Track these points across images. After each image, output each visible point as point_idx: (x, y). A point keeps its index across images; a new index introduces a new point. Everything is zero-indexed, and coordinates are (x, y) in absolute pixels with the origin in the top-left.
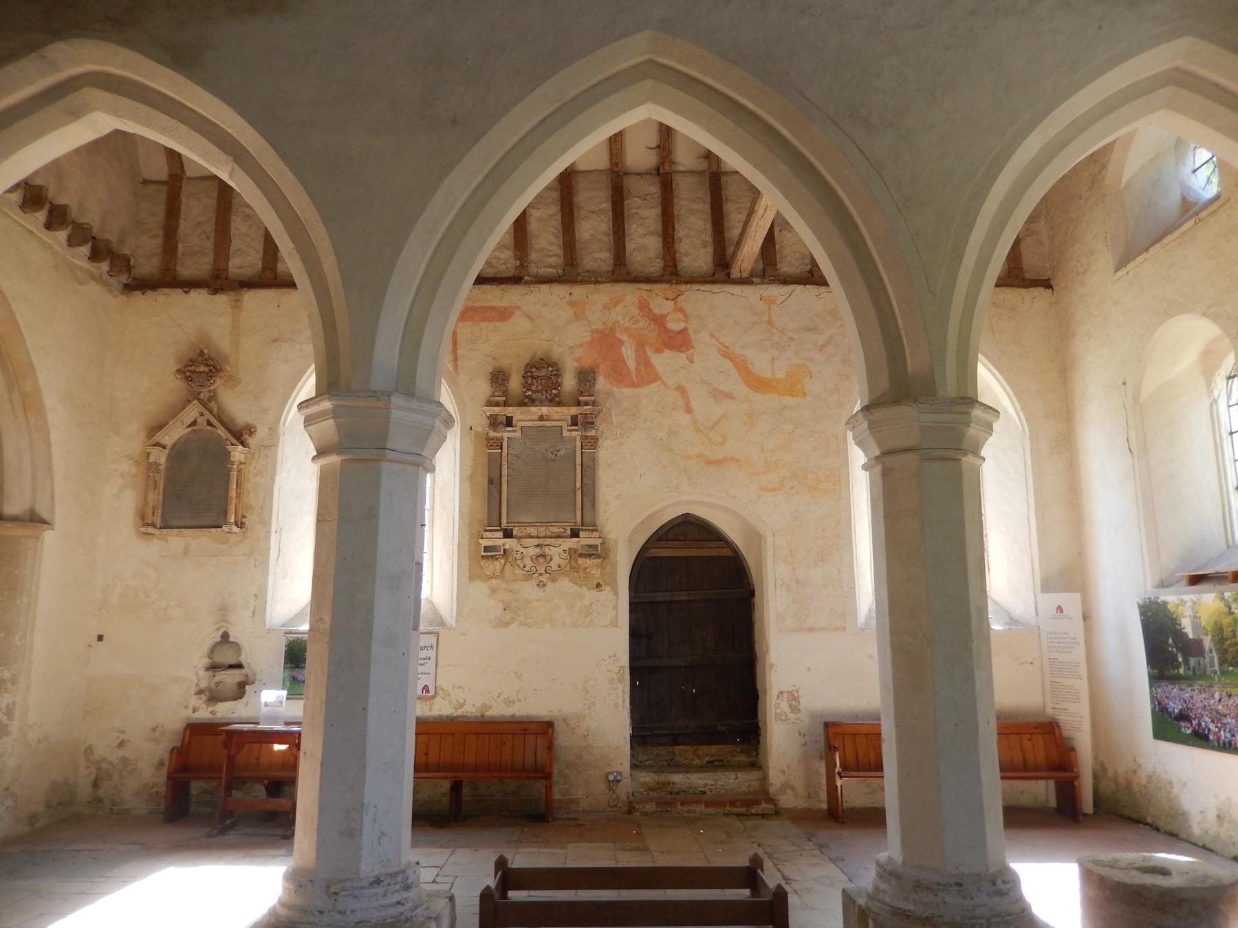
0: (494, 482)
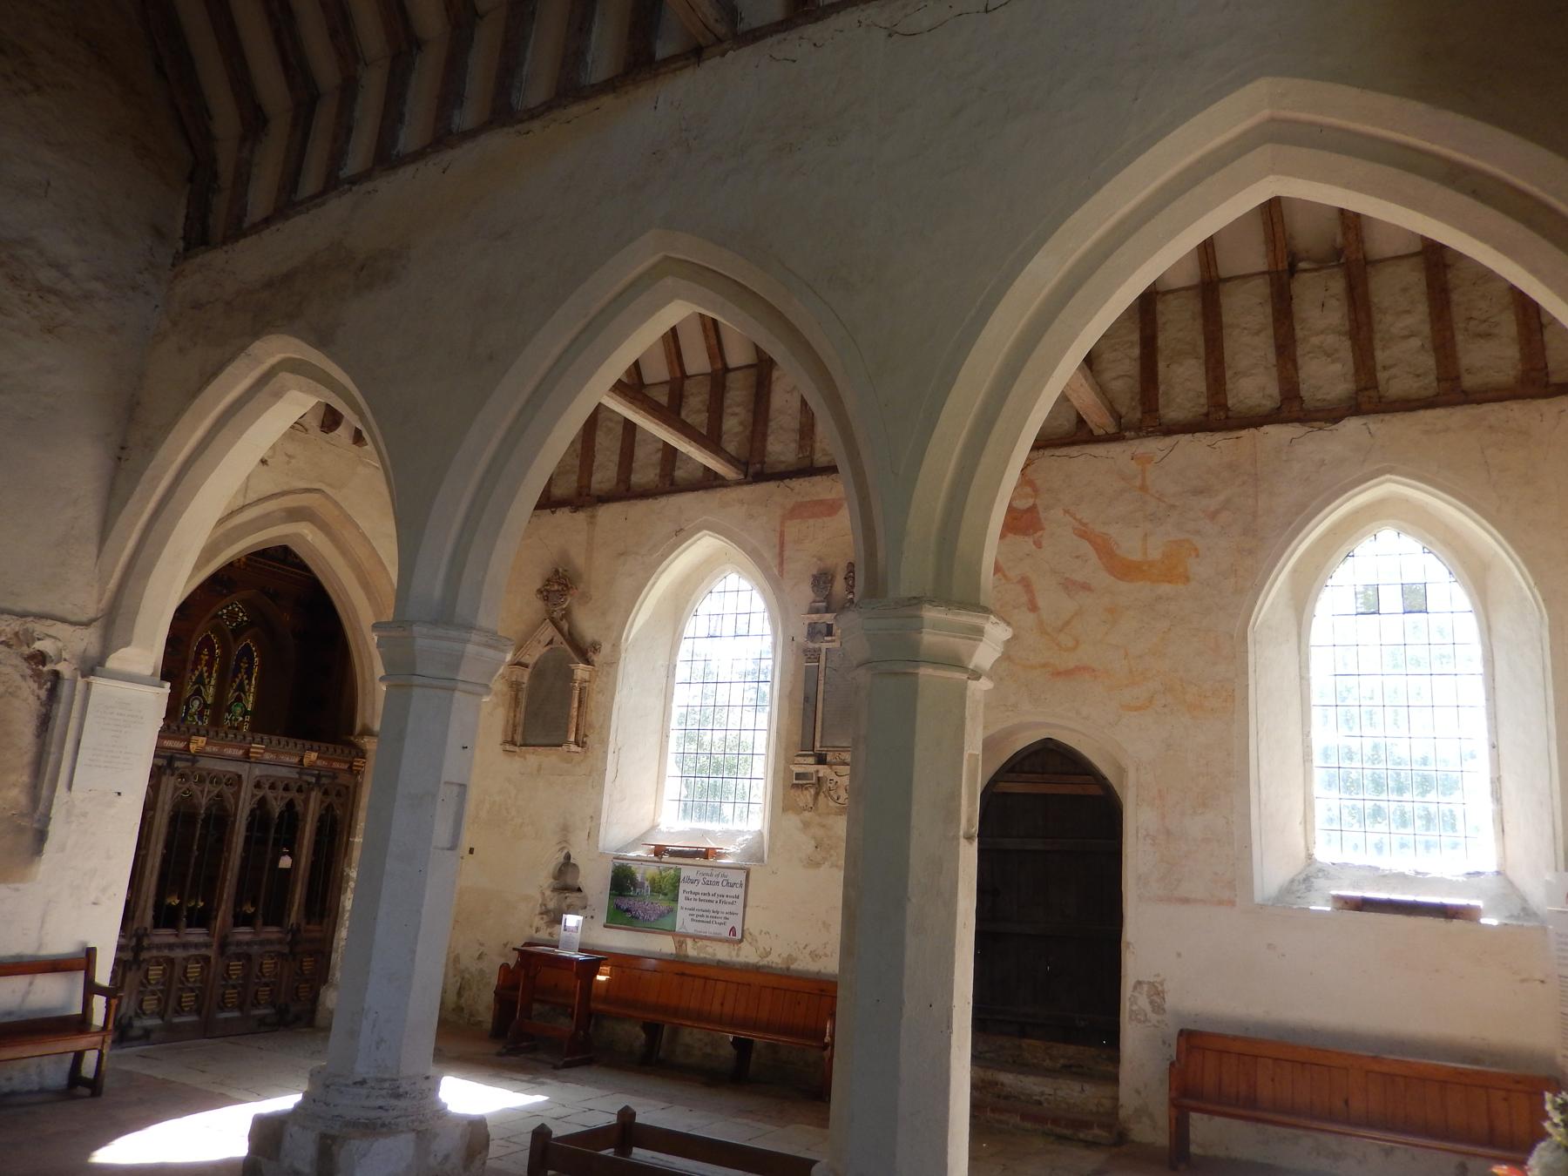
0: (809, 701)
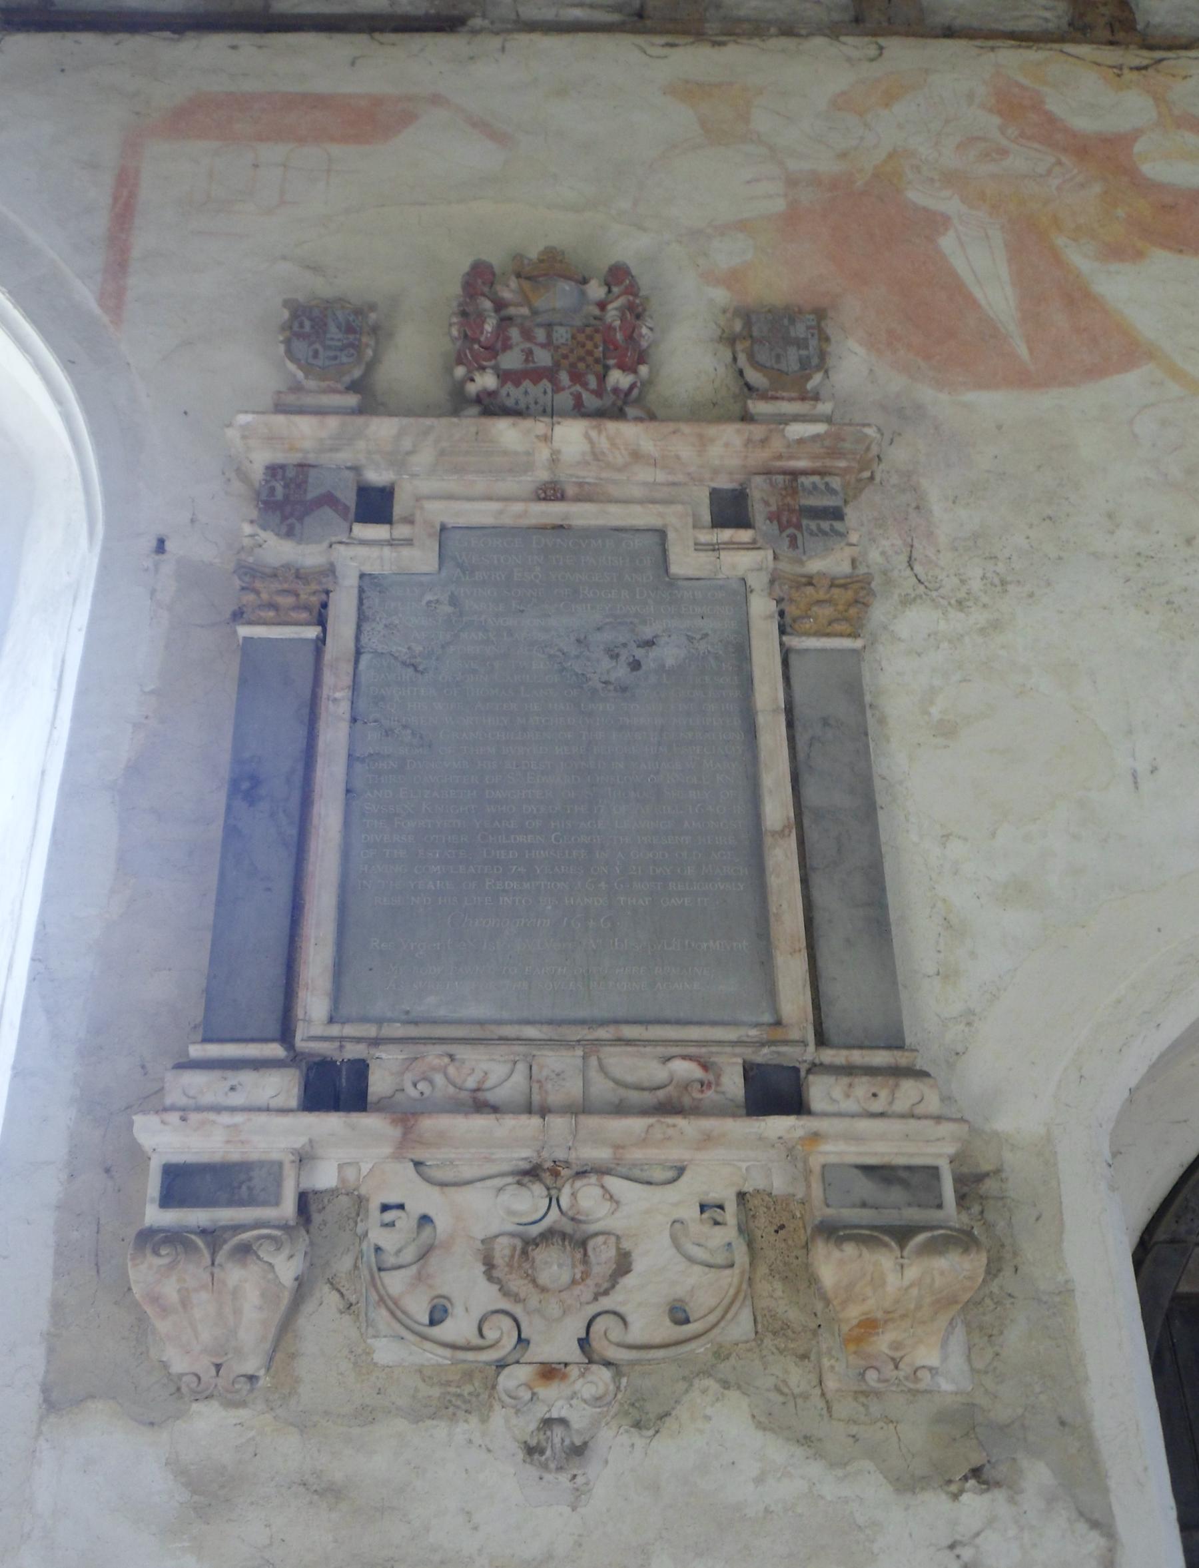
0: (264, 796)
